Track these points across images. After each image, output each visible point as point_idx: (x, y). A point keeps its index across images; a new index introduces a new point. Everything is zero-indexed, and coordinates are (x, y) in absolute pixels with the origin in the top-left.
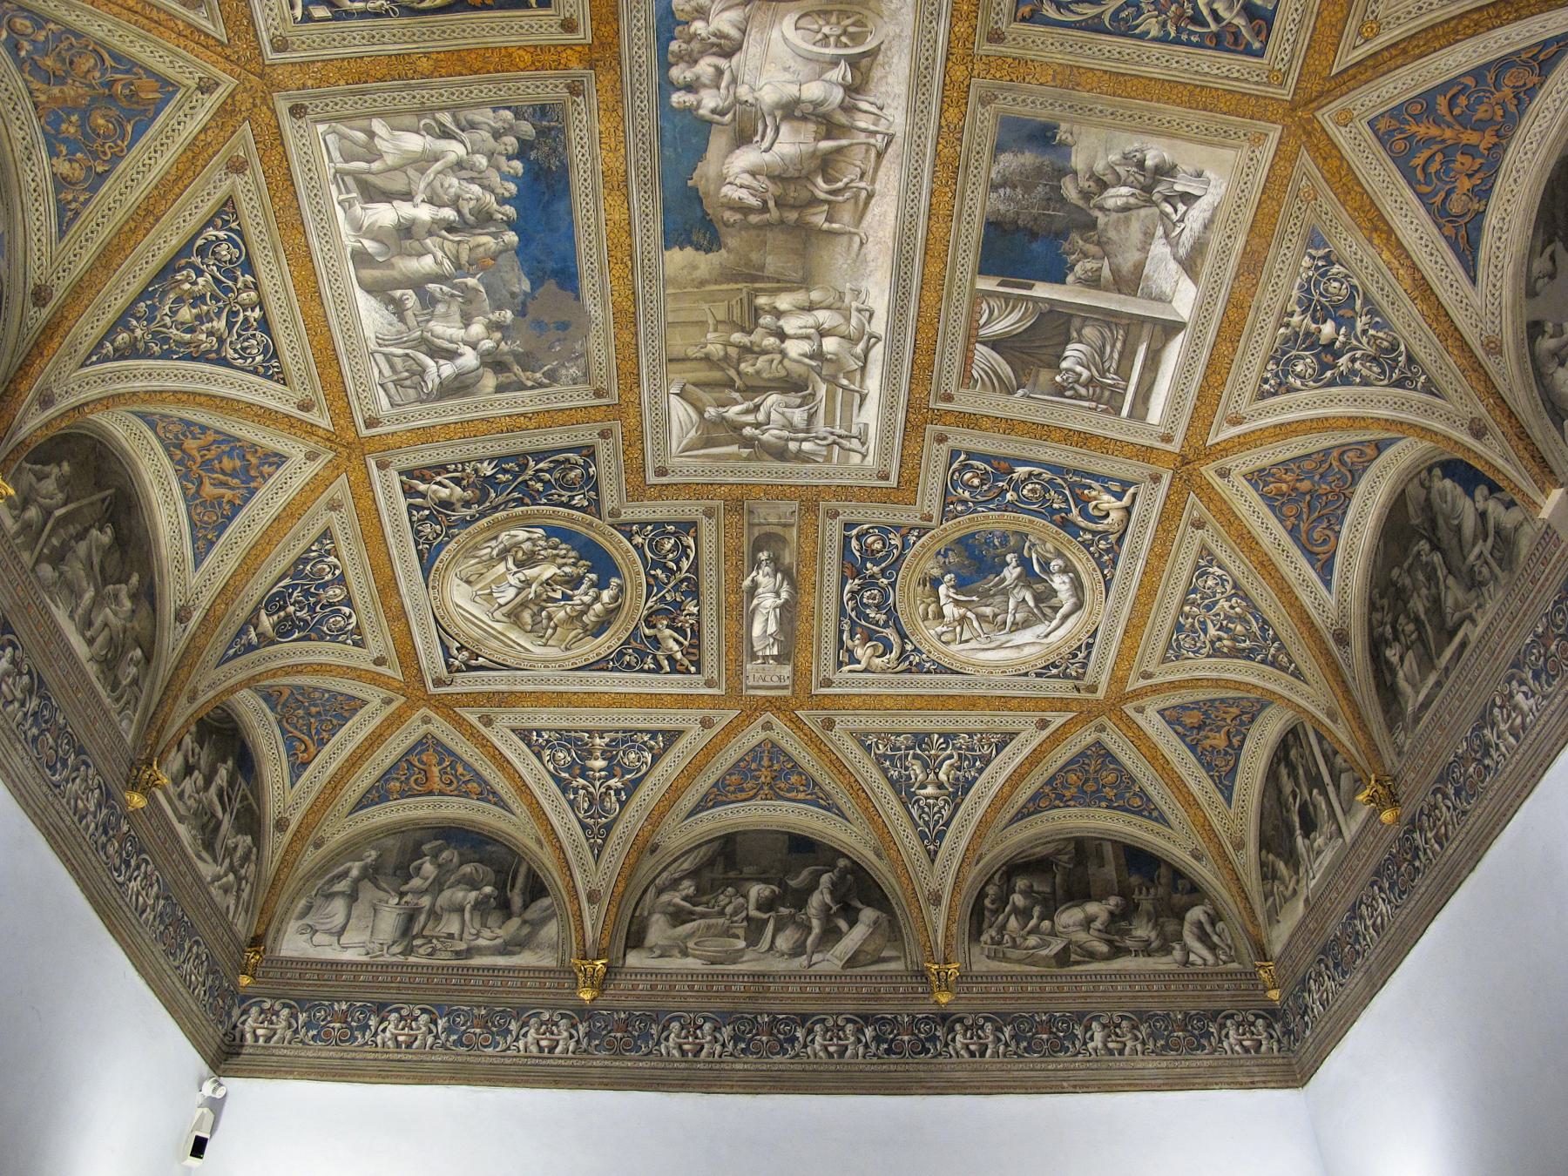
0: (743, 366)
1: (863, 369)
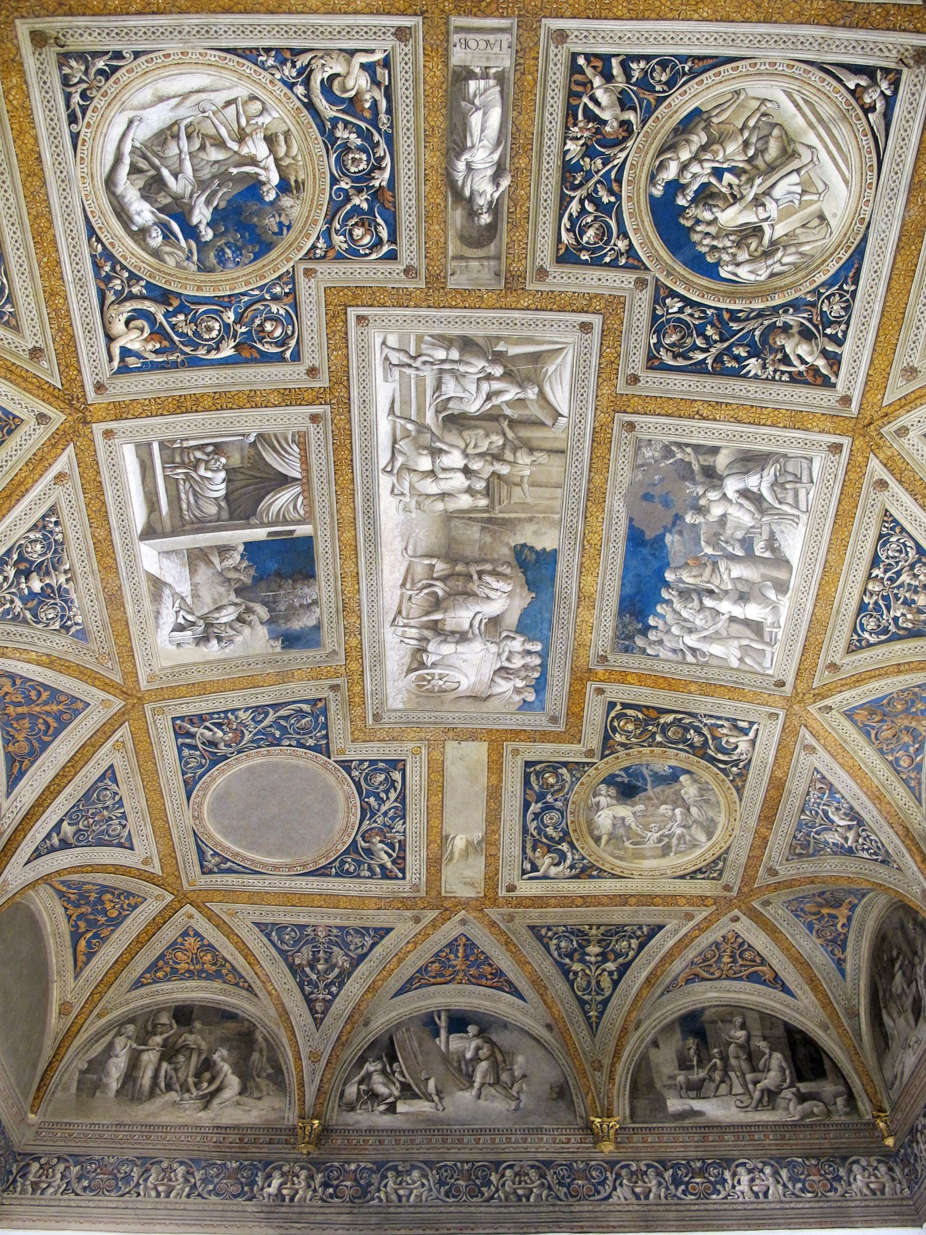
0: (501, 442)
1: (395, 442)
